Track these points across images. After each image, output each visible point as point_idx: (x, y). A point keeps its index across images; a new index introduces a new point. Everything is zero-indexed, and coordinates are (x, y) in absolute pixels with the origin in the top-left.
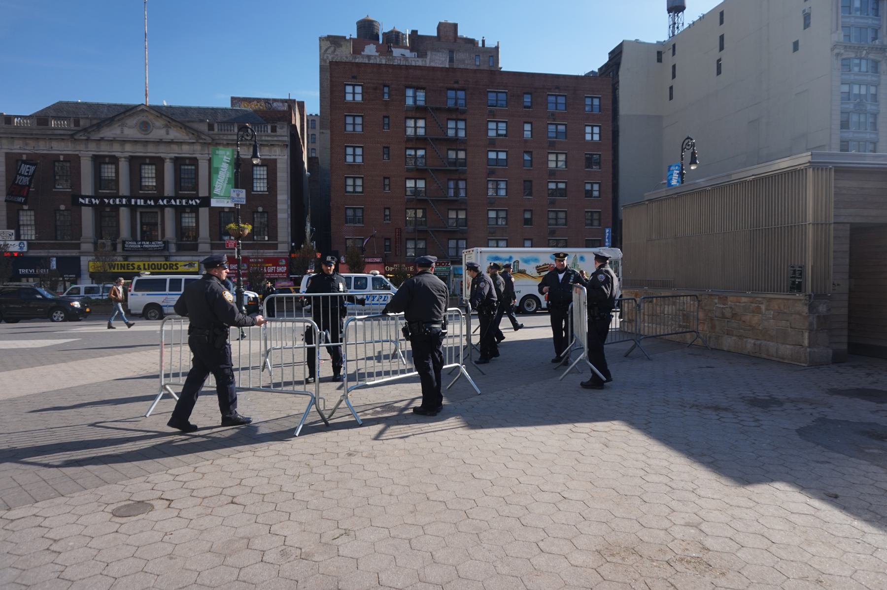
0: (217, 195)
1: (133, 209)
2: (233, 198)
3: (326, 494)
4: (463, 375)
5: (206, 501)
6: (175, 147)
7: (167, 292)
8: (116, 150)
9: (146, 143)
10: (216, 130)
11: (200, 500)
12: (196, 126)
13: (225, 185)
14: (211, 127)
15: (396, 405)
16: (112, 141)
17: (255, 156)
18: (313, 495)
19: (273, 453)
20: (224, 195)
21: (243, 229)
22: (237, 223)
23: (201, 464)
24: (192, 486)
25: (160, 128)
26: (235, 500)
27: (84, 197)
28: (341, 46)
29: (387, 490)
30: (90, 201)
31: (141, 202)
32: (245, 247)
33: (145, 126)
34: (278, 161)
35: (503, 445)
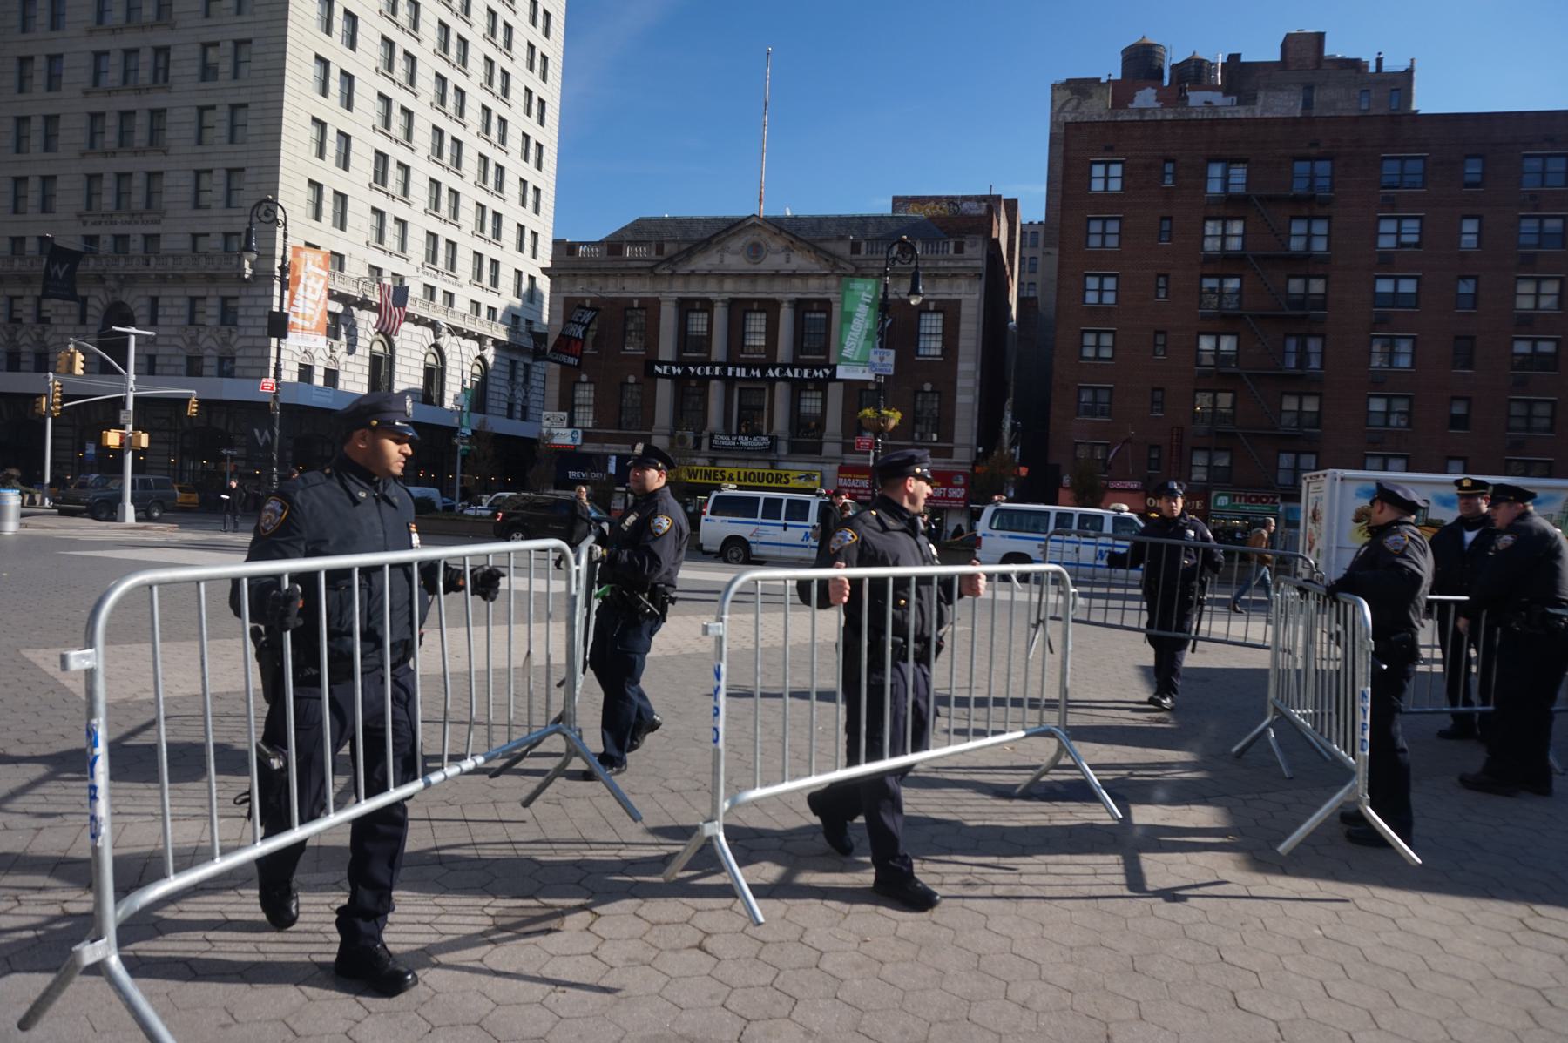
0: (847, 359)
1: (729, 382)
2: (873, 365)
3: (887, 971)
5: (656, 931)
6: (797, 282)
7: (759, 519)
8: (711, 290)
9: (754, 277)
10: (863, 253)
11: (646, 926)
12: (830, 246)
13: (861, 343)
14: (855, 248)
16: (707, 275)
17: (914, 291)
18: (858, 966)
20: (858, 355)
21: (886, 419)
25: (777, 253)
26: (708, 943)
27: (661, 364)
28: (1090, 96)
29: (1021, 992)
30: (670, 371)
31: (741, 372)
33: (755, 251)
35: (1328, 930)
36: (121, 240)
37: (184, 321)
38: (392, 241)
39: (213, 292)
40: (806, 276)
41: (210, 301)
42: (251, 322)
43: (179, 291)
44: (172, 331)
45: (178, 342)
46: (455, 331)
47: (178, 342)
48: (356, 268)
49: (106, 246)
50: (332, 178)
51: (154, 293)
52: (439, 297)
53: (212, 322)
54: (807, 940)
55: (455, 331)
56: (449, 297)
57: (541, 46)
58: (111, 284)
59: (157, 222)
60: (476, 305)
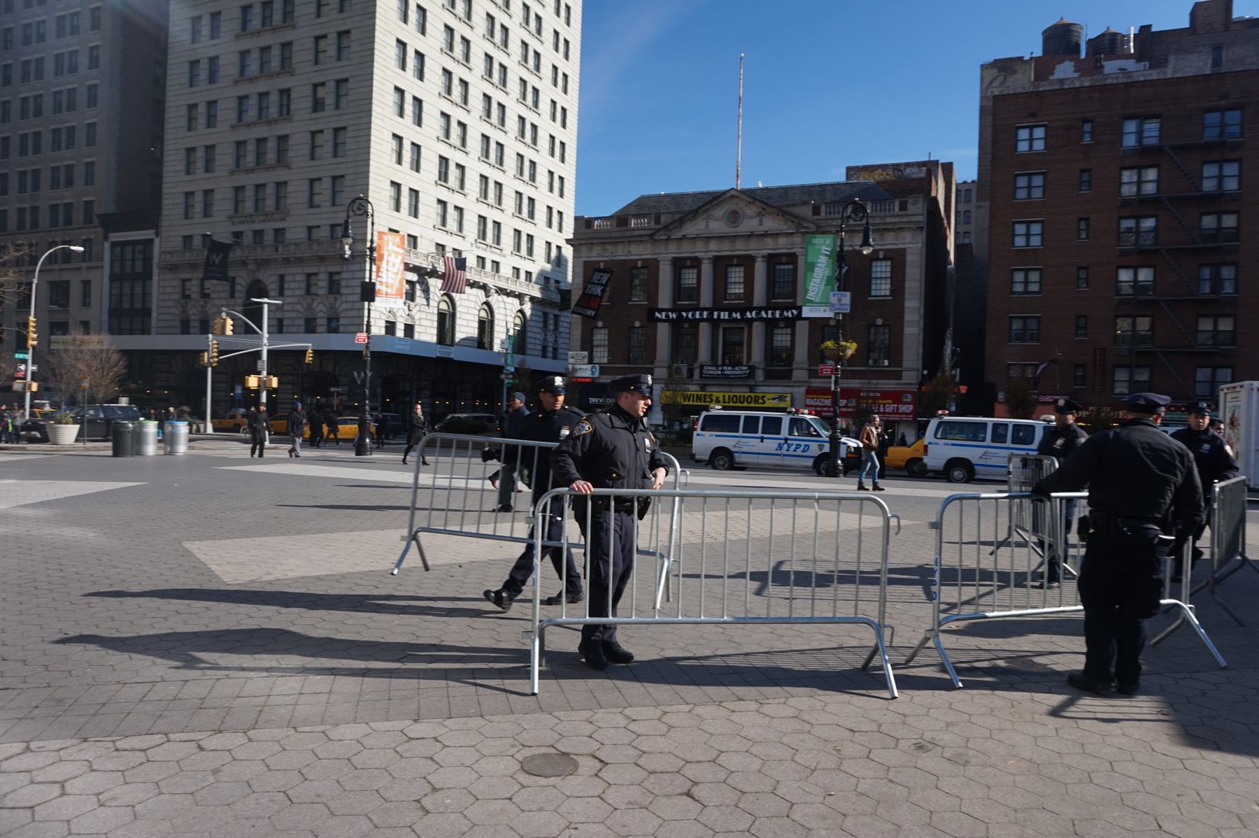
0: (811, 301)
1: (715, 323)
2: (833, 305)
3: (849, 822)
4: (1187, 622)
6: (769, 241)
7: (740, 433)
8: (699, 250)
9: (733, 238)
10: (823, 214)
11: (644, 774)
12: (795, 210)
13: (822, 287)
14: (816, 211)
15: (1038, 660)
16: (696, 238)
17: (866, 243)
18: (824, 818)
19: (790, 712)
20: (820, 298)
21: (844, 349)
22: (837, 341)
23: (675, 708)
24: (644, 744)
25: (752, 218)
26: (696, 791)
27: (660, 311)
28: (1015, 72)
30: (667, 316)
31: (725, 315)
32: (846, 374)
33: (734, 217)
34: (908, 251)
36: (258, 234)
37: (302, 292)
38: (452, 224)
39: (322, 269)
40: (775, 235)
41: (322, 276)
42: (350, 291)
43: (299, 270)
44: (295, 300)
45: (299, 307)
46: (501, 291)
47: (299, 307)
48: (426, 246)
49: (248, 239)
50: (408, 179)
51: (281, 272)
52: (488, 265)
53: (322, 292)
54: (778, 792)
55: (501, 291)
56: (496, 264)
57: (563, 67)
58: (252, 266)
59: (283, 220)
60: (517, 270)
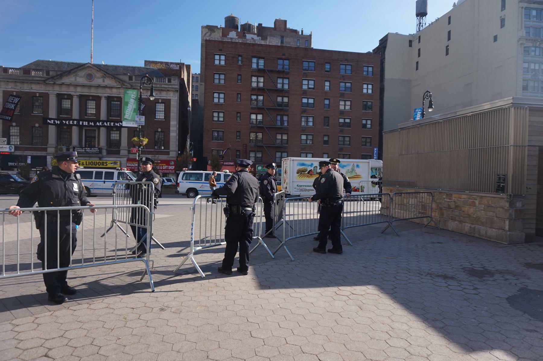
0: (127, 119)
1: (81, 127)
2: (136, 121)
3: (127, 349)
5: (25, 353)
6: (108, 90)
7: (93, 179)
8: (71, 91)
9: (90, 87)
10: (134, 80)
12: (121, 77)
13: (132, 113)
14: (131, 78)
16: (69, 85)
17: (152, 95)
19: (104, 305)
20: (131, 118)
21: (142, 141)
22: (139, 137)
23: (43, 315)
24: (22, 336)
25: (99, 78)
26: (50, 354)
27: (50, 119)
28: (215, 32)
29: (177, 347)
30: (54, 122)
31: (86, 123)
32: (143, 152)
33: (90, 77)
34: (172, 100)
35: (281, 305)
54: (94, 343)
